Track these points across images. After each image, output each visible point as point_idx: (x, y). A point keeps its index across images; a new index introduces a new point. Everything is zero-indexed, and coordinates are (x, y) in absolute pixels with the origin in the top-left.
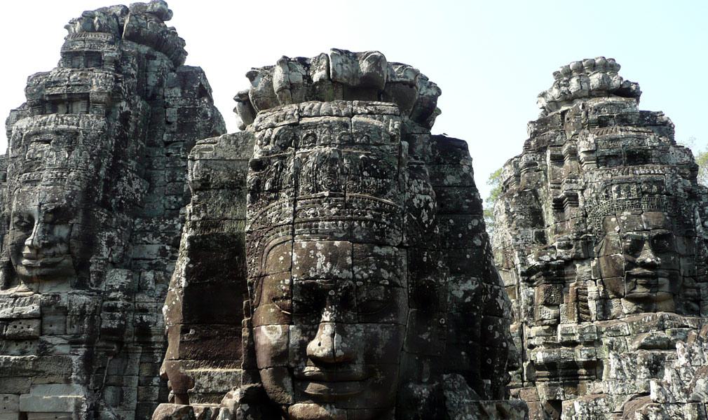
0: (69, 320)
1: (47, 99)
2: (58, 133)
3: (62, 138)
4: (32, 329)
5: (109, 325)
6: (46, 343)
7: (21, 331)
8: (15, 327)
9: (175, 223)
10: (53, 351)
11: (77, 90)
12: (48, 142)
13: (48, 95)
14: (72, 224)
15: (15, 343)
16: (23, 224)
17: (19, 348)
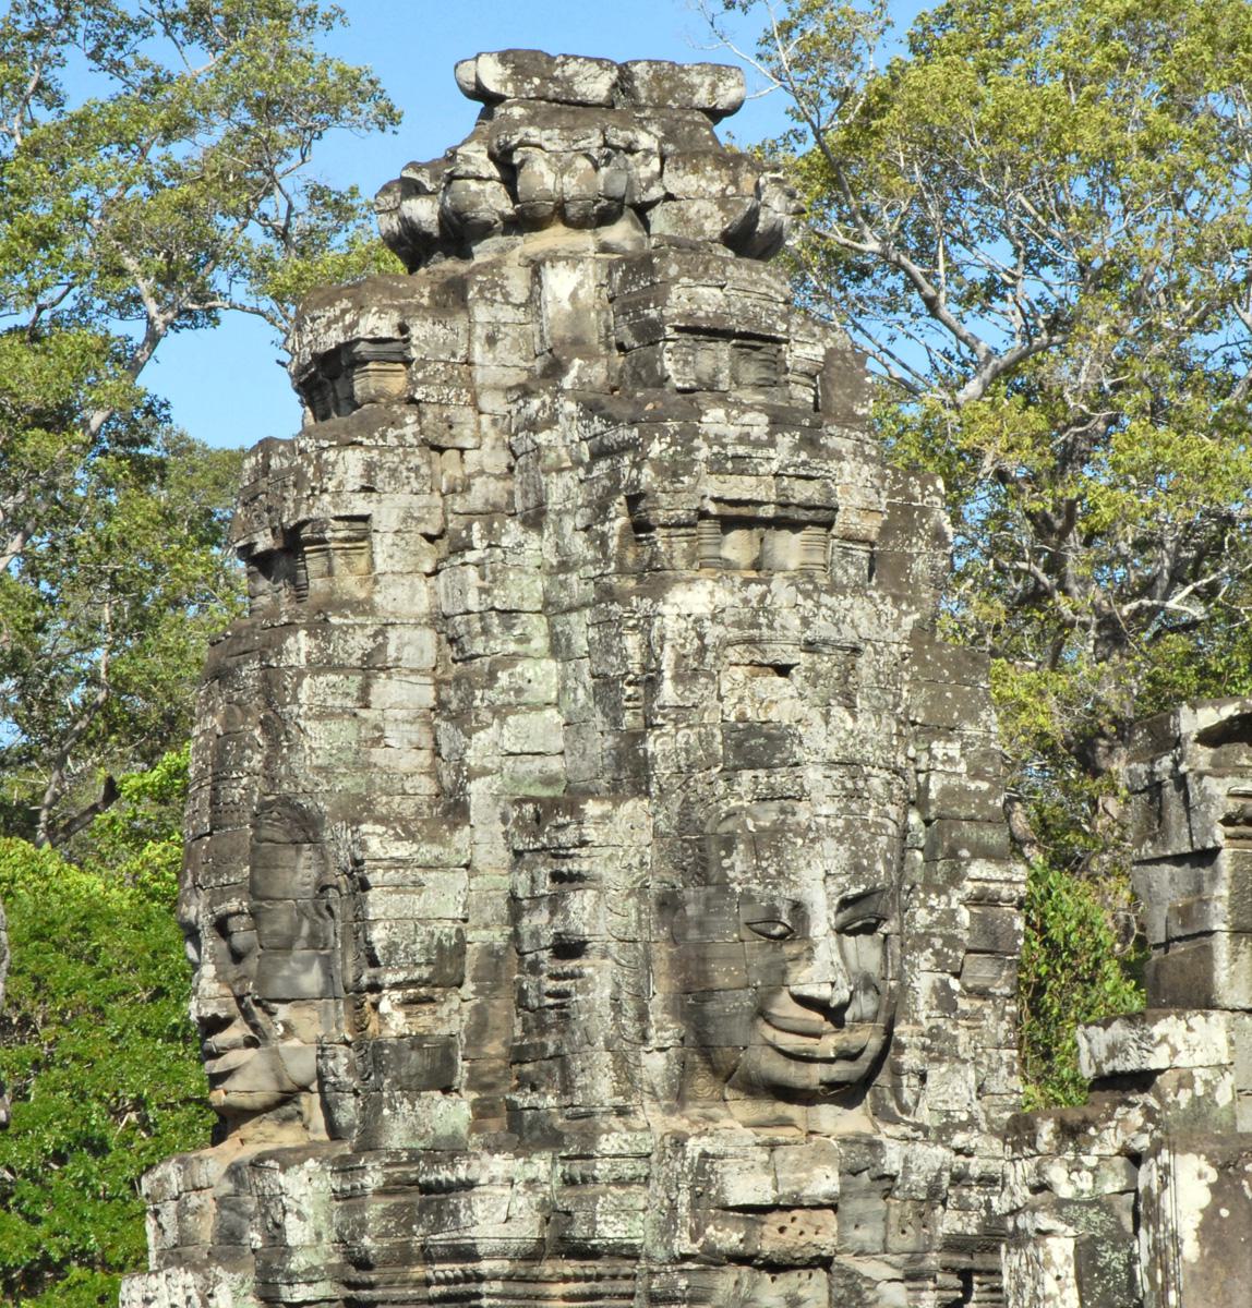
0: (895, 1212)
1: (712, 508)
2: (810, 647)
3: (825, 664)
4: (823, 1234)
5: (959, 1227)
6: (860, 1275)
7: (802, 1241)
8: (782, 1230)
9: (954, 905)
10: (876, 1301)
11: (804, 492)
12: (783, 670)
13: (717, 500)
14: (886, 936)
15: (767, 1277)
16: (779, 929)
17: (785, 1290)
